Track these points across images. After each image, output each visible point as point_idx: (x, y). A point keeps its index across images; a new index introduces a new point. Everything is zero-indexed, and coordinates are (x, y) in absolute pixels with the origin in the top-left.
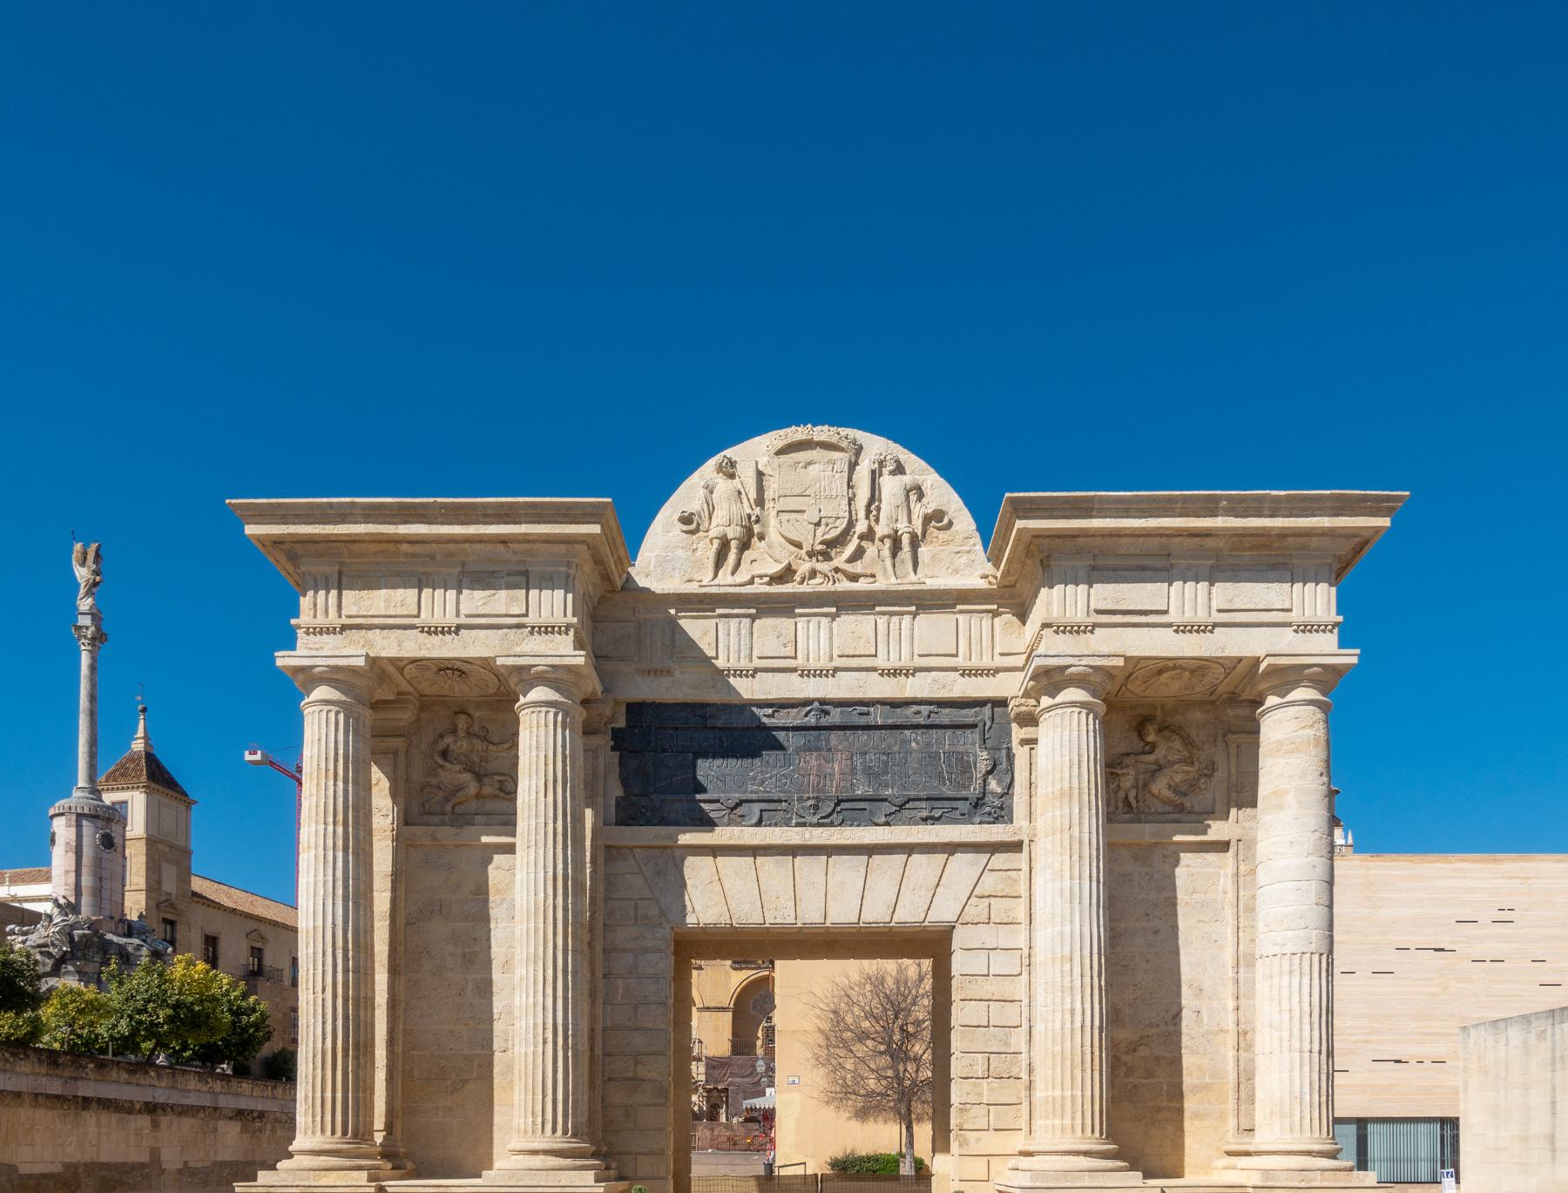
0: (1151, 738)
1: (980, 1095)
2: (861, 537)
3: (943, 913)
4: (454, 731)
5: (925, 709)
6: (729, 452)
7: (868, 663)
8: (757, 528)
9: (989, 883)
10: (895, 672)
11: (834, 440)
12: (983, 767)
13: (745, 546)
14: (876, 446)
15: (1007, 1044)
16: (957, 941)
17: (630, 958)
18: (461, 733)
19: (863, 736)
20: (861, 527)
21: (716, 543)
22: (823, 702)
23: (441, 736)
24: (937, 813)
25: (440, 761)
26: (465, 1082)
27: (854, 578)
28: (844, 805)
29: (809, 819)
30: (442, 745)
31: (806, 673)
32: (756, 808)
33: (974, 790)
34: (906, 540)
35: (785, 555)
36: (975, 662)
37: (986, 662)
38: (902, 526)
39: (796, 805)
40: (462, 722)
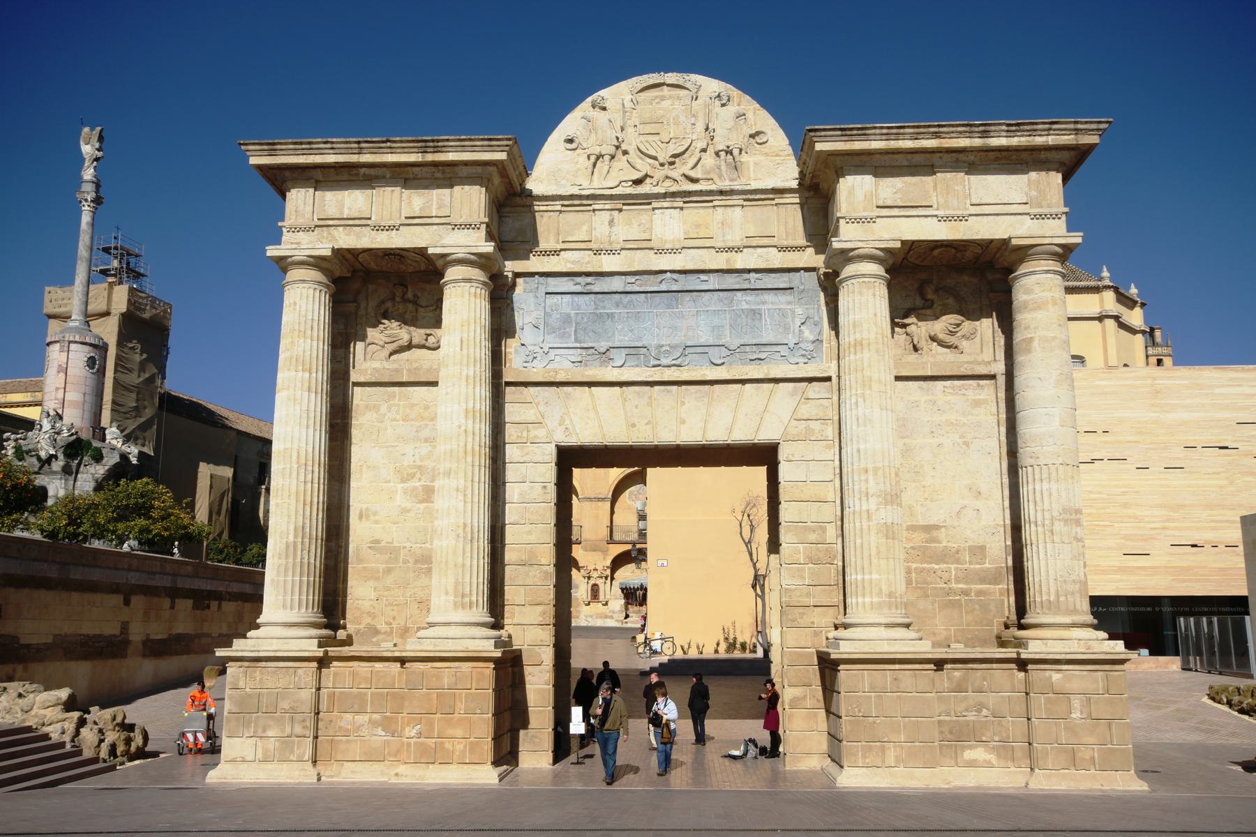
0: (930, 296)
2: (704, 150)
4: (393, 299)
6: (602, 93)
7: (708, 243)
8: (624, 147)
9: (805, 410)
10: (730, 249)
11: (681, 83)
13: (613, 157)
14: (711, 85)
16: (782, 456)
18: (398, 299)
20: (701, 145)
21: (593, 158)
23: (383, 302)
24: (762, 356)
27: (694, 181)
28: (688, 350)
29: (664, 361)
31: (660, 251)
34: (736, 152)
35: (644, 166)
36: (790, 242)
40: (399, 292)
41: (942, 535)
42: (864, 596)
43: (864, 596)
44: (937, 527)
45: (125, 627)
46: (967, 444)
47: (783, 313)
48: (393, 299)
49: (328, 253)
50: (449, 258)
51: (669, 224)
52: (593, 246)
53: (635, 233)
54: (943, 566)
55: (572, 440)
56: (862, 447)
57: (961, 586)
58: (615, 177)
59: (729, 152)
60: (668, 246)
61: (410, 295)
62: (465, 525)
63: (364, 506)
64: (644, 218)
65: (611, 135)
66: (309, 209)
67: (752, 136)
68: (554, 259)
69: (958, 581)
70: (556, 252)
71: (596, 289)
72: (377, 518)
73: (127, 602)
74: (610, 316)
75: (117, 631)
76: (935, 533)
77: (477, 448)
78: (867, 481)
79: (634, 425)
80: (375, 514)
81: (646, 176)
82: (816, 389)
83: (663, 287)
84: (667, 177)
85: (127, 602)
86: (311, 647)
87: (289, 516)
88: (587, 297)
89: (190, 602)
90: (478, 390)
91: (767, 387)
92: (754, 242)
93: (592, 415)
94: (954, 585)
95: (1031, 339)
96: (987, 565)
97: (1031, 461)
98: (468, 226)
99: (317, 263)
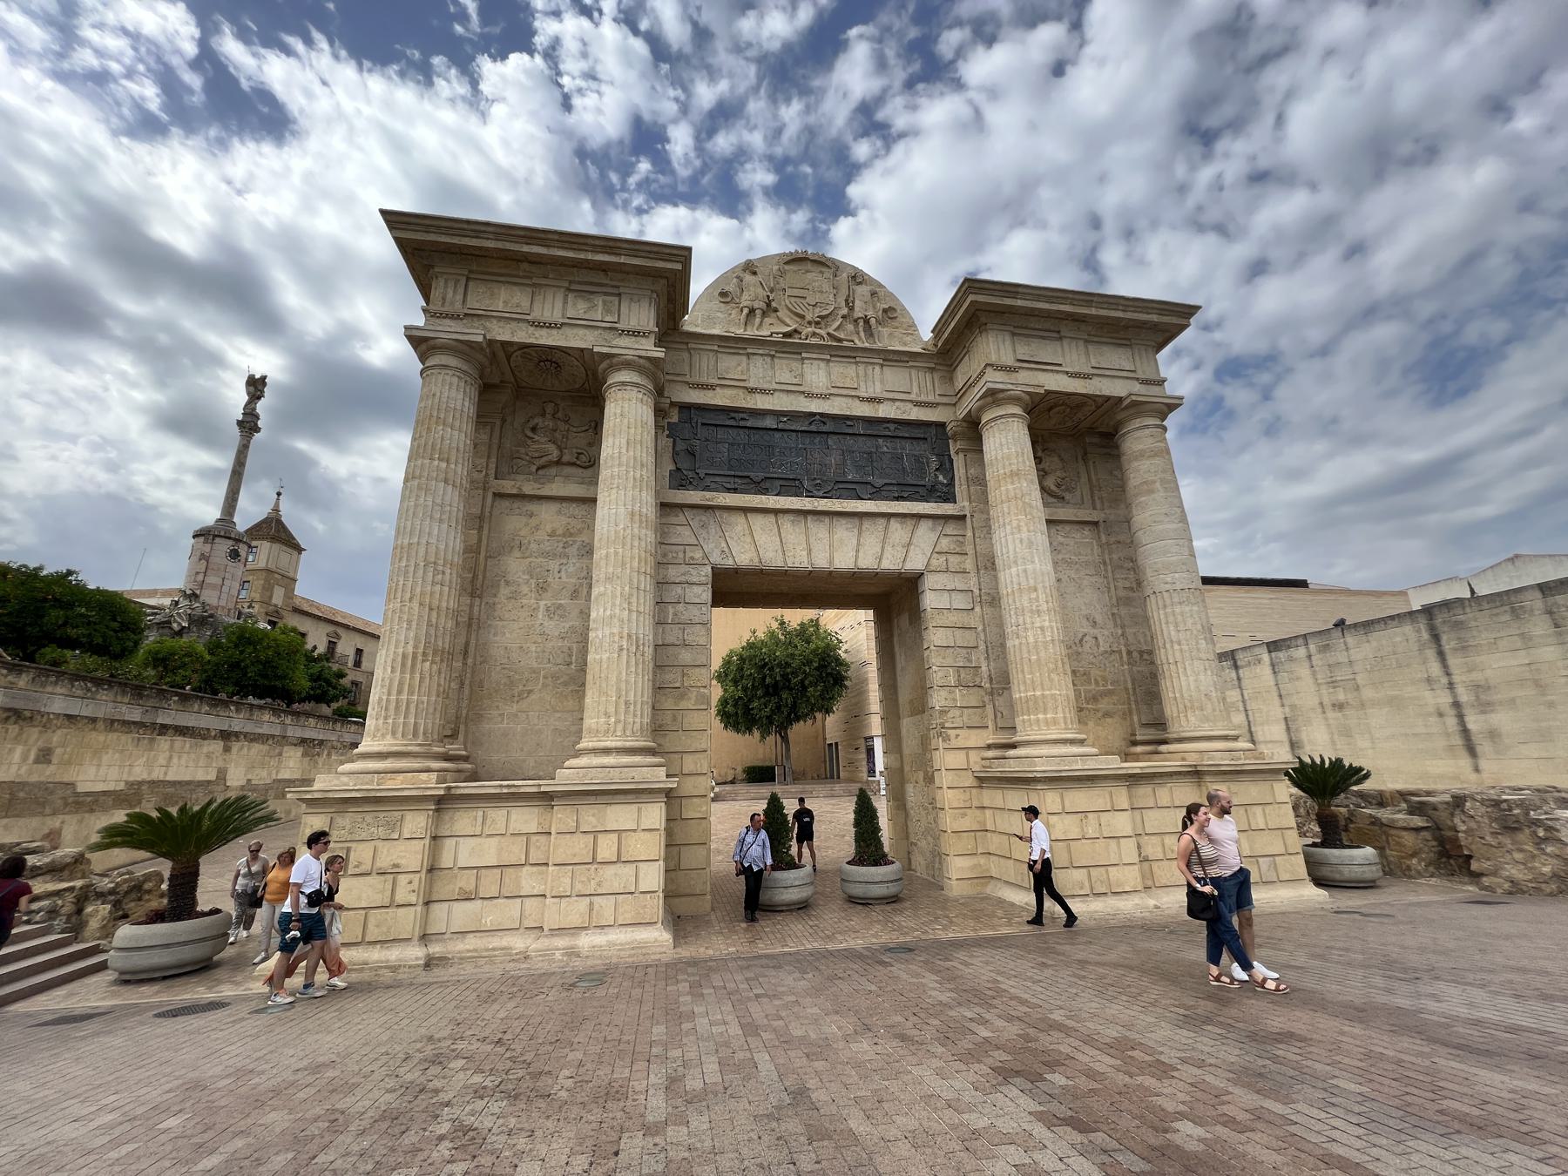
1: (955, 700)
2: (844, 317)
3: (915, 563)
4: (543, 415)
5: (892, 427)
8: (774, 304)
9: (945, 543)
10: (871, 400)
12: (934, 466)
13: (764, 314)
15: (970, 661)
17: (679, 590)
19: (850, 441)
21: (746, 311)
22: (821, 415)
25: (530, 434)
26: (530, 692)
30: (531, 424)
31: (809, 395)
32: (779, 483)
33: (927, 481)
34: (873, 321)
36: (923, 398)
37: (931, 398)
38: (870, 313)
39: (806, 484)
42: (1045, 712)
43: (1045, 712)
45: (222, 774)
47: (917, 459)
48: (543, 415)
49: (480, 339)
50: (615, 360)
51: (817, 375)
52: (751, 384)
53: (785, 376)
55: (729, 563)
56: (1030, 567)
58: (767, 329)
59: (867, 321)
60: (815, 391)
61: (560, 415)
62: (629, 636)
64: (795, 365)
65: (762, 293)
66: (459, 297)
67: (885, 311)
68: (710, 393)
70: (711, 387)
71: (749, 424)
73: (227, 749)
75: (212, 776)
78: (1037, 599)
81: (795, 331)
82: (950, 529)
83: (813, 428)
84: (814, 334)
85: (227, 749)
86: (429, 783)
87: (409, 622)
88: (741, 431)
89: (299, 751)
91: (910, 523)
92: (891, 396)
93: (749, 539)
97: (1168, 587)
98: (635, 333)
99: (464, 349)
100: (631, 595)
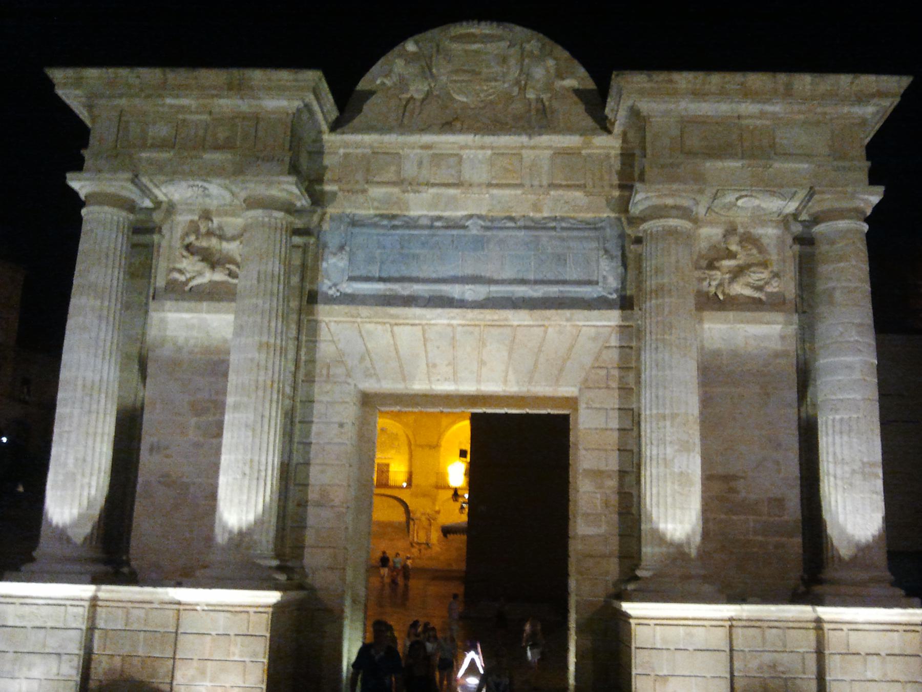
41: (740, 484)
44: (734, 478)
46: (768, 394)
54: (743, 517)
57: (760, 538)
63: (155, 439)
69: (756, 533)
72: (168, 452)
74: (415, 257)
76: (733, 484)
77: (269, 383)
79: (435, 366)
80: (167, 448)
90: (273, 324)
94: (751, 537)
95: (834, 288)
96: (786, 518)
100: (255, 421)
